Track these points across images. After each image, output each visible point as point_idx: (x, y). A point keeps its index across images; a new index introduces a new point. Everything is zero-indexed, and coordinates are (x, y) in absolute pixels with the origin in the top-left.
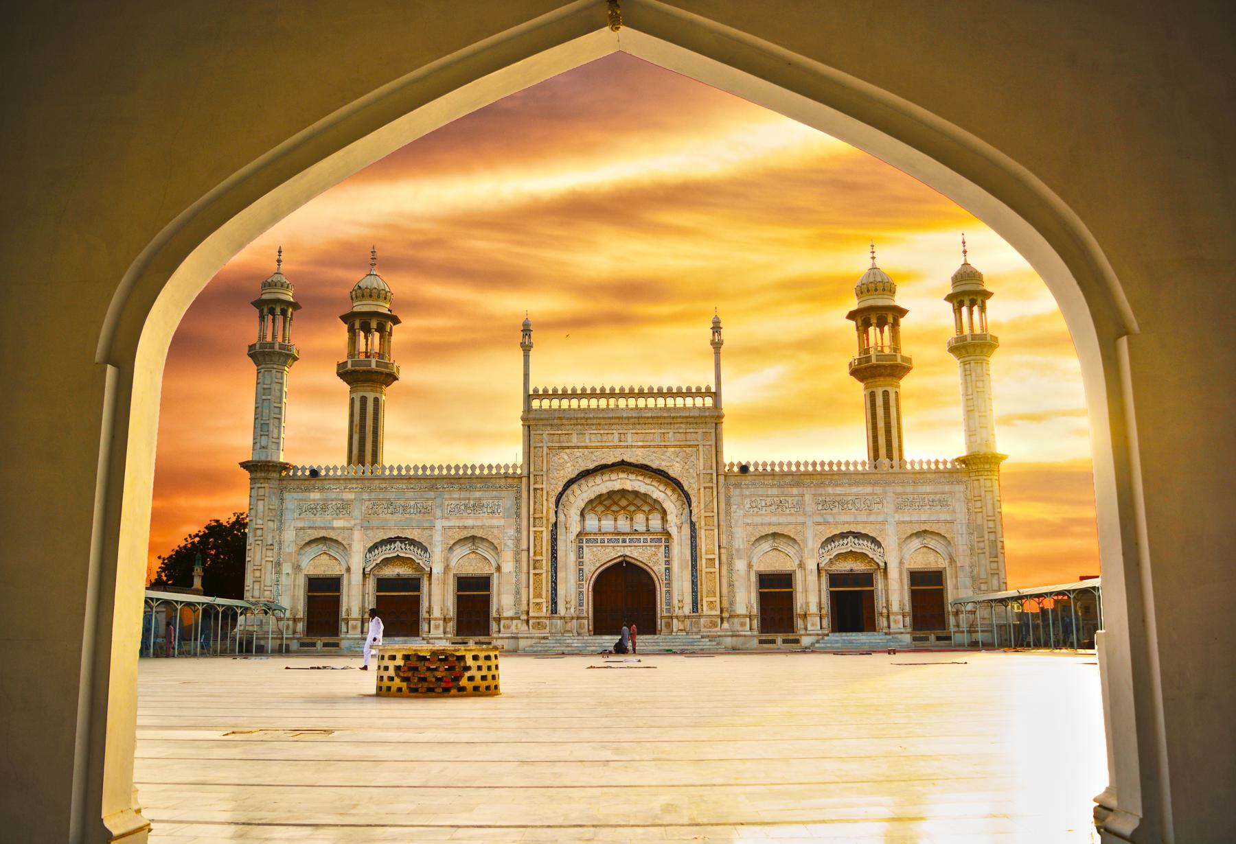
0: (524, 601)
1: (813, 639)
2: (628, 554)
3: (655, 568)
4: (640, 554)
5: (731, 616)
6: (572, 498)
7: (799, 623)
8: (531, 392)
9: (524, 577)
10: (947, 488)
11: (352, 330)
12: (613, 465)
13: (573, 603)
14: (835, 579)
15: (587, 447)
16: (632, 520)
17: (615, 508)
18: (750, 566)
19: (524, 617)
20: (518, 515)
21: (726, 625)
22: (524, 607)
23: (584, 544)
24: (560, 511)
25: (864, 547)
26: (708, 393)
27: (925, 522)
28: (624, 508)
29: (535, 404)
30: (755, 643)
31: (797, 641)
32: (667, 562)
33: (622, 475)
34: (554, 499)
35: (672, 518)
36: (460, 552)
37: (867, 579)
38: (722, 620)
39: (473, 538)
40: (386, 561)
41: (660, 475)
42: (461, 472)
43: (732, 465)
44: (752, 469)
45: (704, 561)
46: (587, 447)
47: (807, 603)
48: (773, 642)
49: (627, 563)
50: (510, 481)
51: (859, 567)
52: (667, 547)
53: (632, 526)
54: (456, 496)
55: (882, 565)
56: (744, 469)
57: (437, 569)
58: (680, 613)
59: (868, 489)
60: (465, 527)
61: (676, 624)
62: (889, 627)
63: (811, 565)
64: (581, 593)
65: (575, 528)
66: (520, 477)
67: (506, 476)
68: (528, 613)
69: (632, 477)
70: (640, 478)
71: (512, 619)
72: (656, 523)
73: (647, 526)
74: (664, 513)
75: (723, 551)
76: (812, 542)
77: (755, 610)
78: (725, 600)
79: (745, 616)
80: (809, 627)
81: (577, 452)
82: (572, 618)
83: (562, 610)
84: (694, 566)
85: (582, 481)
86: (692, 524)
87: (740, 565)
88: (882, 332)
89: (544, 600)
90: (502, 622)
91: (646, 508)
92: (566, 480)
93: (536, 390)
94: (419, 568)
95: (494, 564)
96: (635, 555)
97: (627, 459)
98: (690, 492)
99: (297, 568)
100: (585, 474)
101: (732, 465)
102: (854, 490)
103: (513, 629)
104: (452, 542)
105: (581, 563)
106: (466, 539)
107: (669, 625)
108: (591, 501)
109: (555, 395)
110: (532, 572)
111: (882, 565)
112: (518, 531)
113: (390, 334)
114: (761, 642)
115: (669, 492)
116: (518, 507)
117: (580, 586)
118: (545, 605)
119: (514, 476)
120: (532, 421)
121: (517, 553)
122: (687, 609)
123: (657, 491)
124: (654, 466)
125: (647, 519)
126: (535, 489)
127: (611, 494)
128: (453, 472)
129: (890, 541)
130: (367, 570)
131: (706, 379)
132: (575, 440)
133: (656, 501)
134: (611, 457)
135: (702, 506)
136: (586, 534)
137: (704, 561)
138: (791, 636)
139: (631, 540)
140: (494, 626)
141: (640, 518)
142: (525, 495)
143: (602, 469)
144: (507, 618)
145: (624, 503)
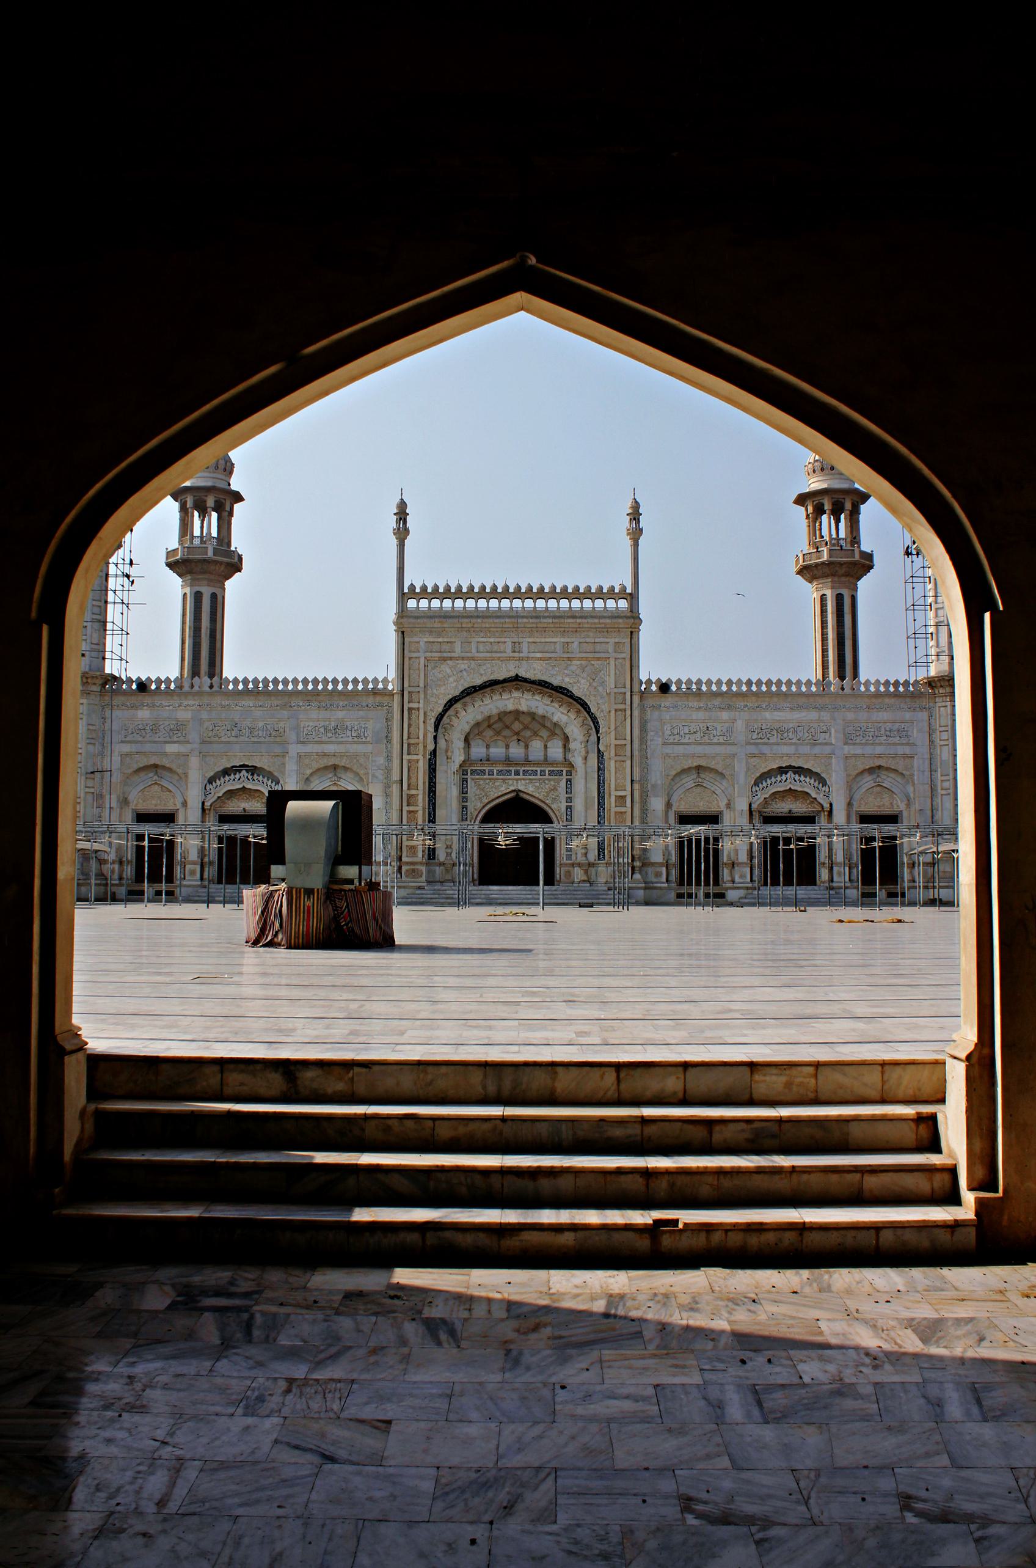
1: (742, 893)
2: (521, 788)
3: (554, 806)
4: (533, 789)
5: (644, 865)
6: (455, 721)
8: (406, 590)
10: (908, 715)
11: (183, 509)
12: (505, 681)
13: (455, 846)
15: (473, 659)
16: (527, 746)
17: (506, 732)
18: (669, 805)
20: (389, 740)
21: (637, 876)
23: (469, 776)
24: (440, 735)
25: (805, 784)
26: (623, 594)
27: (879, 757)
28: (517, 734)
29: (412, 603)
31: (722, 896)
32: (569, 800)
33: (516, 694)
34: (431, 722)
35: (576, 745)
38: (633, 868)
39: (335, 767)
40: (231, 794)
41: (562, 693)
43: (649, 682)
44: (674, 688)
46: (473, 659)
50: (379, 699)
51: (799, 808)
52: (569, 781)
55: (826, 806)
56: (664, 688)
59: (813, 715)
60: (325, 755)
62: (832, 881)
63: (742, 805)
65: (459, 757)
66: (391, 694)
67: (375, 692)
68: (400, 859)
69: (528, 696)
70: (538, 697)
72: (556, 751)
74: (566, 739)
75: (636, 786)
76: (743, 778)
79: (661, 865)
80: (737, 879)
81: (463, 665)
83: (441, 855)
84: (601, 805)
85: (467, 699)
86: (600, 754)
87: (657, 804)
88: (838, 521)
91: (544, 733)
93: (412, 587)
96: (530, 789)
97: (523, 673)
98: (598, 715)
99: (124, 802)
100: (470, 692)
102: (797, 715)
104: (308, 772)
106: (326, 768)
107: (569, 874)
108: (478, 724)
109: (435, 593)
110: (405, 808)
111: (826, 806)
112: (389, 758)
113: (231, 514)
115: (572, 715)
116: (389, 729)
120: (407, 624)
121: (387, 786)
124: (555, 682)
125: (546, 747)
126: (410, 709)
127: (502, 715)
129: (836, 779)
130: (207, 804)
134: (503, 672)
137: (613, 799)
139: (525, 773)
143: (491, 685)
145: (517, 726)
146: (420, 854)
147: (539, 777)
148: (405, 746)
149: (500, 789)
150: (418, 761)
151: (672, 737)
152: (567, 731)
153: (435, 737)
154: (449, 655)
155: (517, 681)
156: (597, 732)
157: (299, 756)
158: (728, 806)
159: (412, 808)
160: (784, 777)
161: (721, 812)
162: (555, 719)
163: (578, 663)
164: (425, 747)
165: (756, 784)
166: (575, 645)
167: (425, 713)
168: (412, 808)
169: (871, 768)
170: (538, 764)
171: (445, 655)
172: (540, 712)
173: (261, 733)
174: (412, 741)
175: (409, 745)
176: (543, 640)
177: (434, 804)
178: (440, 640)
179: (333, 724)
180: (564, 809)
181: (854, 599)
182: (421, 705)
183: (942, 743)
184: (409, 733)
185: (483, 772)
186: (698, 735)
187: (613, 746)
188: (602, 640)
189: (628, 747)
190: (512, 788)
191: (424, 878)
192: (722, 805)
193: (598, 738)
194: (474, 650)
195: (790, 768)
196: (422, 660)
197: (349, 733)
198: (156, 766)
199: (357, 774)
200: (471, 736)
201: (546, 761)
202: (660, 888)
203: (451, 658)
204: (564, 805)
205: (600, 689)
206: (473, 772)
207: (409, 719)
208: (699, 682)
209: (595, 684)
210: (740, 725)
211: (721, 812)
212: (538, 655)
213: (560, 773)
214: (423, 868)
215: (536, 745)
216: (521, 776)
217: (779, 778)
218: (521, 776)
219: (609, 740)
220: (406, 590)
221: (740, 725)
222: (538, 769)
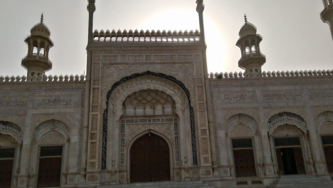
0: (84, 161)
2: (152, 128)
3: (169, 137)
4: (159, 129)
6: (118, 95)
7: (259, 170)
8: (93, 32)
9: (84, 145)
13: (117, 162)
14: (277, 141)
15: (126, 64)
16: (154, 108)
17: (144, 101)
18: (227, 134)
19: (83, 173)
20: (83, 105)
21: (216, 173)
22: (83, 166)
24: (110, 103)
25: (294, 121)
26: (196, 34)
28: (149, 102)
29: (96, 39)
30: (235, 183)
31: (260, 182)
33: (148, 81)
35: (178, 106)
36: (43, 131)
37: (296, 140)
38: (213, 169)
39: (53, 121)
41: (171, 79)
44: (224, 77)
45: (200, 131)
46: (126, 64)
47: (264, 157)
48: (245, 183)
49: (152, 134)
50: (78, 84)
51: (292, 134)
53: (154, 112)
54: (43, 94)
55: (305, 132)
57: (27, 142)
58: (186, 166)
59: (292, 87)
60: (48, 114)
61: (184, 174)
62: (315, 171)
63: (264, 133)
64: (123, 154)
68: (86, 170)
70: (159, 82)
71: (75, 174)
72: (168, 110)
73: (163, 112)
74: (174, 103)
75: (211, 124)
77: (232, 163)
78: (214, 155)
79: (227, 166)
80: (268, 173)
82: (116, 172)
83: (109, 167)
85: (124, 84)
86: (191, 109)
87: (221, 134)
89: (97, 161)
90: (68, 177)
91: (163, 101)
92: (113, 83)
93: (96, 32)
94: (15, 142)
95: (66, 138)
96: (157, 129)
97: (151, 70)
101: (212, 75)
102: (284, 88)
103: (76, 181)
104: (38, 124)
105: (123, 135)
106: (48, 121)
107: (179, 174)
108: (129, 96)
109: (108, 34)
110: (89, 141)
111: (305, 132)
114: (238, 183)
115: (176, 91)
116: (83, 101)
117: (121, 150)
118: (97, 163)
120: (93, 48)
121: (81, 130)
122: (190, 163)
123: (170, 90)
124: (168, 73)
125: (163, 108)
126: (94, 89)
127: (142, 92)
131: (195, 27)
132: (119, 59)
133: (168, 96)
135: (197, 97)
136: (127, 117)
137: (200, 131)
138: (256, 179)
140: (63, 178)
142: (87, 92)
144: (72, 174)
145: (149, 98)
146: (97, 167)
147: (161, 122)
148: (91, 107)
150: (97, 115)
151: (225, 100)
152: (174, 98)
153: (107, 103)
154: (114, 62)
155: (149, 74)
156: (189, 97)
157: (34, 115)
158: (256, 134)
159: (93, 141)
160: (282, 118)
161: (253, 137)
162: (168, 93)
163: (178, 65)
164: (101, 107)
165: (270, 122)
166: (177, 56)
167: (102, 91)
168: (93, 141)
169: (324, 112)
170: (160, 116)
171: (112, 62)
173: (13, 104)
174: (94, 105)
175: (93, 106)
176: (161, 54)
177: (106, 138)
178: (110, 55)
179: (53, 98)
180: (174, 138)
182: (100, 87)
184: (93, 101)
185: (132, 121)
186: (238, 98)
187: (197, 104)
188: (189, 54)
190: (147, 129)
191: (98, 181)
193: (190, 101)
194: (127, 60)
196: (101, 65)
197: (62, 103)
199: (65, 124)
200: (126, 103)
201: (164, 115)
202: (228, 180)
203: (116, 64)
205: (189, 77)
206: (127, 121)
207: (93, 93)
209: (187, 75)
210: (258, 93)
211: (253, 137)
212: (159, 61)
213: (171, 120)
214: (98, 175)
215: (159, 107)
216: (152, 122)
217: (280, 119)
219: (195, 101)
220: (93, 32)
221: (258, 93)
222: (160, 118)
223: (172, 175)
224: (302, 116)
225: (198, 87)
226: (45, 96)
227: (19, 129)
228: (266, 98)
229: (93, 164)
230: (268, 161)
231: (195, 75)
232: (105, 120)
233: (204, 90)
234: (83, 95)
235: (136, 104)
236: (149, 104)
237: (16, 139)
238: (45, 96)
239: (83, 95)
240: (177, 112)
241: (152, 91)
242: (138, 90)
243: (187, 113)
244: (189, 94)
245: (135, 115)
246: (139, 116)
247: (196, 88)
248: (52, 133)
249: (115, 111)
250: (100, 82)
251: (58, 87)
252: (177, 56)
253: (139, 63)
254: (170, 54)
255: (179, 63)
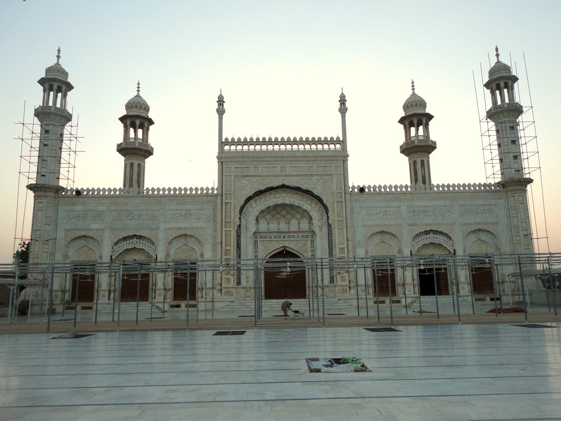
2: (286, 245)
3: (304, 255)
4: (293, 245)
7: (399, 290)
8: (224, 141)
10: (493, 202)
16: (289, 224)
17: (278, 216)
18: (367, 253)
19: (219, 288)
20: (215, 221)
23: (258, 240)
25: (440, 239)
26: (338, 141)
27: (479, 224)
28: (284, 216)
29: (227, 148)
31: (399, 302)
32: (313, 251)
33: (283, 195)
36: (177, 244)
38: (350, 288)
39: (185, 235)
40: (127, 251)
41: (308, 193)
42: (177, 192)
44: (367, 190)
45: (337, 249)
49: (287, 251)
50: (209, 198)
52: (312, 241)
53: (289, 228)
54: (174, 208)
56: (362, 190)
59: (442, 203)
60: (180, 229)
63: (407, 253)
65: (253, 229)
66: (216, 196)
67: (207, 195)
68: (221, 285)
69: (289, 195)
70: (294, 196)
72: (305, 225)
73: (299, 227)
74: (311, 218)
75: (349, 242)
81: (254, 179)
82: (251, 288)
85: (257, 198)
86: (329, 226)
91: (298, 216)
93: (227, 139)
94: (149, 255)
95: (199, 253)
96: (292, 246)
97: (286, 183)
98: (328, 205)
99: (66, 256)
100: (259, 193)
101: (353, 187)
102: (432, 203)
104: (171, 238)
105: (256, 252)
106: (180, 236)
108: (263, 211)
109: (239, 142)
111: (452, 251)
115: (314, 205)
116: (215, 215)
119: (213, 195)
120: (225, 160)
121: (214, 245)
124: (304, 188)
125: (299, 223)
126: (226, 203)
127: (276, 207)
128: (172, 192)
130: (114, 257)
131: (337, 133)
132: (252, 172)
133: (305, 211)
135: (336, 213)
137: (337, 249)
138: (395, 299)
139: (289, 237)
141: (294, 222)
145: (284, 213)
146: (232, 282)
148: (224, 223)
149: (276, 246)
151: (367, 216)
152: (311, 214)
153: (240, 218)
154: (247, 174)
156: (327, 214)
157: (166, 229)
159: (227, 257)
160: (428, 236)
162: (304, 208)
163: (316, 177)
166: (315, 167)
167: (234, 205)
171: (245, 174)
172: (296, 204)
175: (226, 222)
176: (297, 166)
177: (240, 254)
178: (242, 166)
179: (184, 212)
181: (428, 162)
182: (232, 201)
183: (513, 216)
184: (226, 216)
185: (266, 237)
186: (381, 215)
189: (345, 222)
190: (282, 245)
192: (395, 252)
193: (328, 218)
194: (260, 172)
195: (431, 230)
196: (233, 177)
197: (193, 217)
198: (85, 236)
200: (259, 218)
203: (248, 176)
204: (309, 255)
205: (328, 191)
206: (261, 237)
207: (226, 208)
208: (380, 187)
209: (325, 189)
210: (403, 209)
212: (295, 174)
216: (287, 239)
218: (287, 239)
221: (403, 209)
223: (307, 293)
224: (449, 235)
225: (337, 202)
226: (176, 210)
227: (153, 243)
228: (411, 215)
229: (228, 280)
230: (409, 280)
231: (335, 189)
232: (239, 236)
233: (344, 205)
234: (215, 210)
235: (270, 218)
236: (283, 218)
237: (150, 253)
238: (176, 210)
239: (215, 210)
240: (314, 229)
241: (287, 205)
242: (272, 205)
243: (325, 229)
244: (327, 209)
245: (268, 230)
246: (273, 232)
247: (335, 203)
248: (185, 247)
249: (248, 227)
250: (232, 196)
251: (189, 201)
252: (315, 167)
253: (274, 176)
254: (307, 165)
255: (317, 175)
